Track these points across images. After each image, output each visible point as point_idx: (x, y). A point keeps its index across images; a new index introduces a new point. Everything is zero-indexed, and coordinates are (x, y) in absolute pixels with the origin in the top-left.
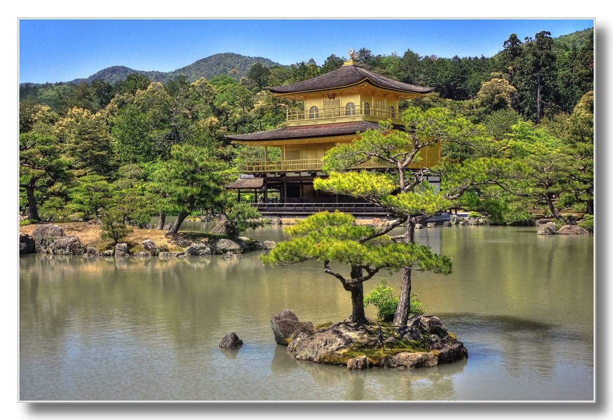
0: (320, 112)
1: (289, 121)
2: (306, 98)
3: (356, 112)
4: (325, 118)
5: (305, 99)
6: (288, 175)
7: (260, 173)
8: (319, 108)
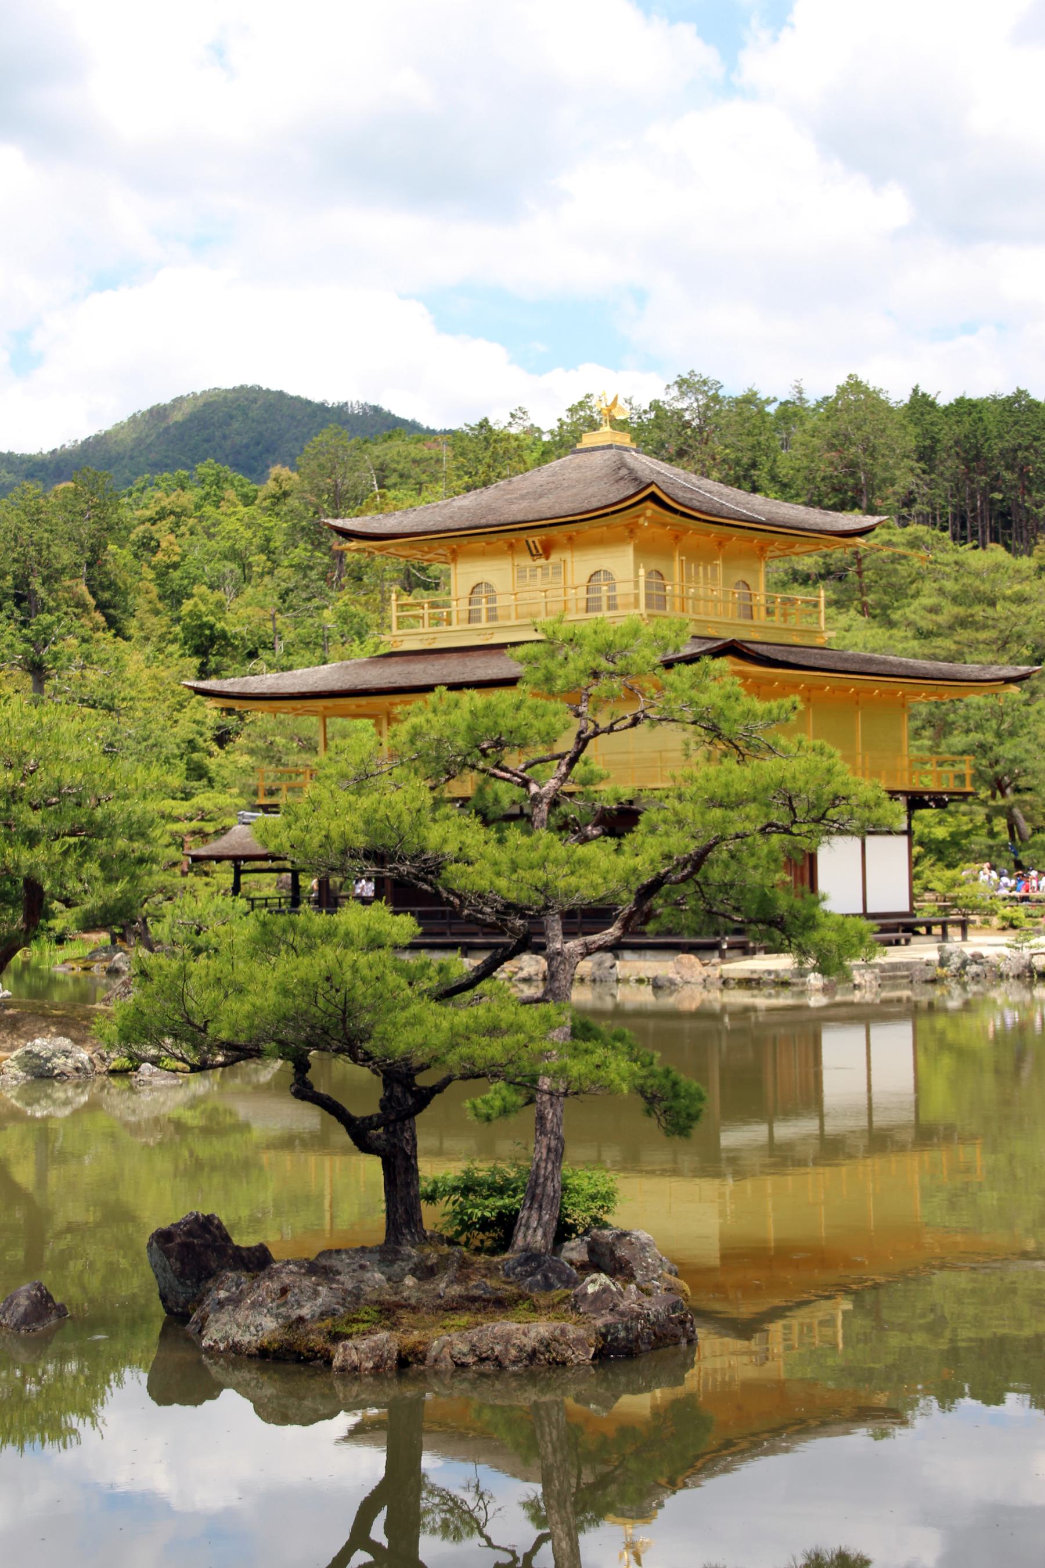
0: (501, 601)
1: (400, 632)
2: (455, 556)
3: (619, 601)
4: (518, 622)
5: (454, 560)
8: (498, 588)
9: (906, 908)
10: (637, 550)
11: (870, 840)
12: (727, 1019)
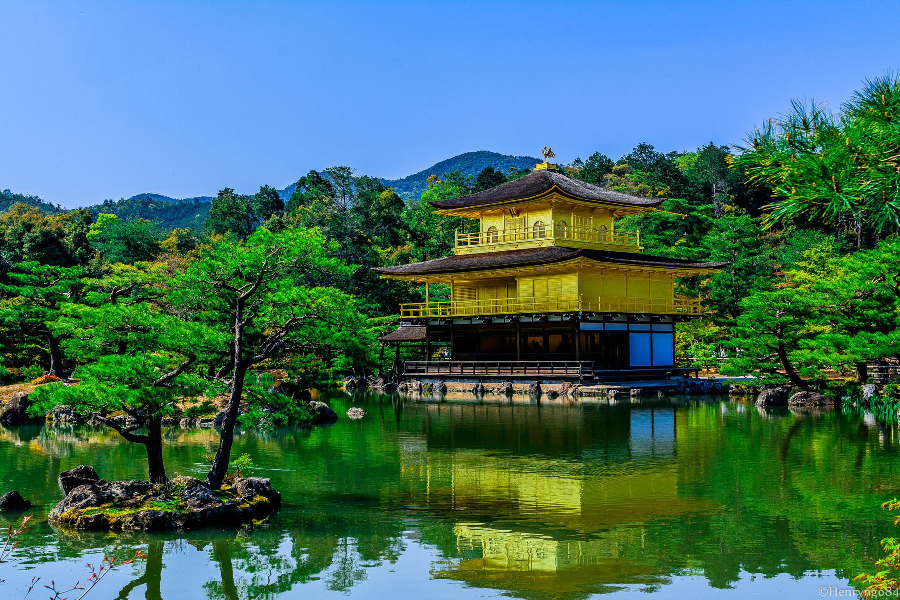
0: (501, 234)
2: (483, 215)
6: (456, 323)
7: (419, 320)
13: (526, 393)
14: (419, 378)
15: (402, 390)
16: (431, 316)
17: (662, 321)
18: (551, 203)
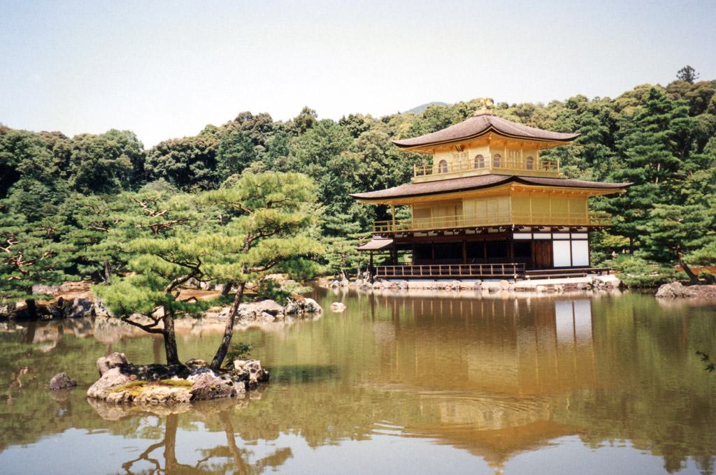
0: (449, 165)
6: (416, 235)
9: (587, 264)
10: (491, 148)
11: (573, 242)
12: (516, 301)
13: (472, 289)
14: (388, 279)
15: (375, 288)
16: (394, 230)
17: (579, 230)
18: (489, 142)
